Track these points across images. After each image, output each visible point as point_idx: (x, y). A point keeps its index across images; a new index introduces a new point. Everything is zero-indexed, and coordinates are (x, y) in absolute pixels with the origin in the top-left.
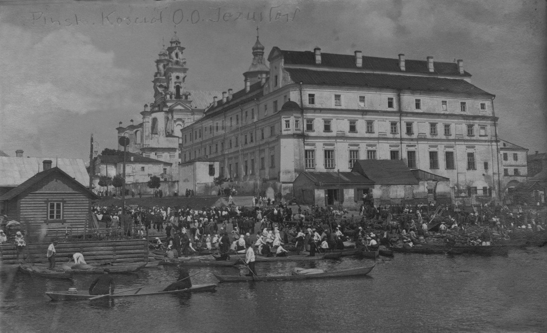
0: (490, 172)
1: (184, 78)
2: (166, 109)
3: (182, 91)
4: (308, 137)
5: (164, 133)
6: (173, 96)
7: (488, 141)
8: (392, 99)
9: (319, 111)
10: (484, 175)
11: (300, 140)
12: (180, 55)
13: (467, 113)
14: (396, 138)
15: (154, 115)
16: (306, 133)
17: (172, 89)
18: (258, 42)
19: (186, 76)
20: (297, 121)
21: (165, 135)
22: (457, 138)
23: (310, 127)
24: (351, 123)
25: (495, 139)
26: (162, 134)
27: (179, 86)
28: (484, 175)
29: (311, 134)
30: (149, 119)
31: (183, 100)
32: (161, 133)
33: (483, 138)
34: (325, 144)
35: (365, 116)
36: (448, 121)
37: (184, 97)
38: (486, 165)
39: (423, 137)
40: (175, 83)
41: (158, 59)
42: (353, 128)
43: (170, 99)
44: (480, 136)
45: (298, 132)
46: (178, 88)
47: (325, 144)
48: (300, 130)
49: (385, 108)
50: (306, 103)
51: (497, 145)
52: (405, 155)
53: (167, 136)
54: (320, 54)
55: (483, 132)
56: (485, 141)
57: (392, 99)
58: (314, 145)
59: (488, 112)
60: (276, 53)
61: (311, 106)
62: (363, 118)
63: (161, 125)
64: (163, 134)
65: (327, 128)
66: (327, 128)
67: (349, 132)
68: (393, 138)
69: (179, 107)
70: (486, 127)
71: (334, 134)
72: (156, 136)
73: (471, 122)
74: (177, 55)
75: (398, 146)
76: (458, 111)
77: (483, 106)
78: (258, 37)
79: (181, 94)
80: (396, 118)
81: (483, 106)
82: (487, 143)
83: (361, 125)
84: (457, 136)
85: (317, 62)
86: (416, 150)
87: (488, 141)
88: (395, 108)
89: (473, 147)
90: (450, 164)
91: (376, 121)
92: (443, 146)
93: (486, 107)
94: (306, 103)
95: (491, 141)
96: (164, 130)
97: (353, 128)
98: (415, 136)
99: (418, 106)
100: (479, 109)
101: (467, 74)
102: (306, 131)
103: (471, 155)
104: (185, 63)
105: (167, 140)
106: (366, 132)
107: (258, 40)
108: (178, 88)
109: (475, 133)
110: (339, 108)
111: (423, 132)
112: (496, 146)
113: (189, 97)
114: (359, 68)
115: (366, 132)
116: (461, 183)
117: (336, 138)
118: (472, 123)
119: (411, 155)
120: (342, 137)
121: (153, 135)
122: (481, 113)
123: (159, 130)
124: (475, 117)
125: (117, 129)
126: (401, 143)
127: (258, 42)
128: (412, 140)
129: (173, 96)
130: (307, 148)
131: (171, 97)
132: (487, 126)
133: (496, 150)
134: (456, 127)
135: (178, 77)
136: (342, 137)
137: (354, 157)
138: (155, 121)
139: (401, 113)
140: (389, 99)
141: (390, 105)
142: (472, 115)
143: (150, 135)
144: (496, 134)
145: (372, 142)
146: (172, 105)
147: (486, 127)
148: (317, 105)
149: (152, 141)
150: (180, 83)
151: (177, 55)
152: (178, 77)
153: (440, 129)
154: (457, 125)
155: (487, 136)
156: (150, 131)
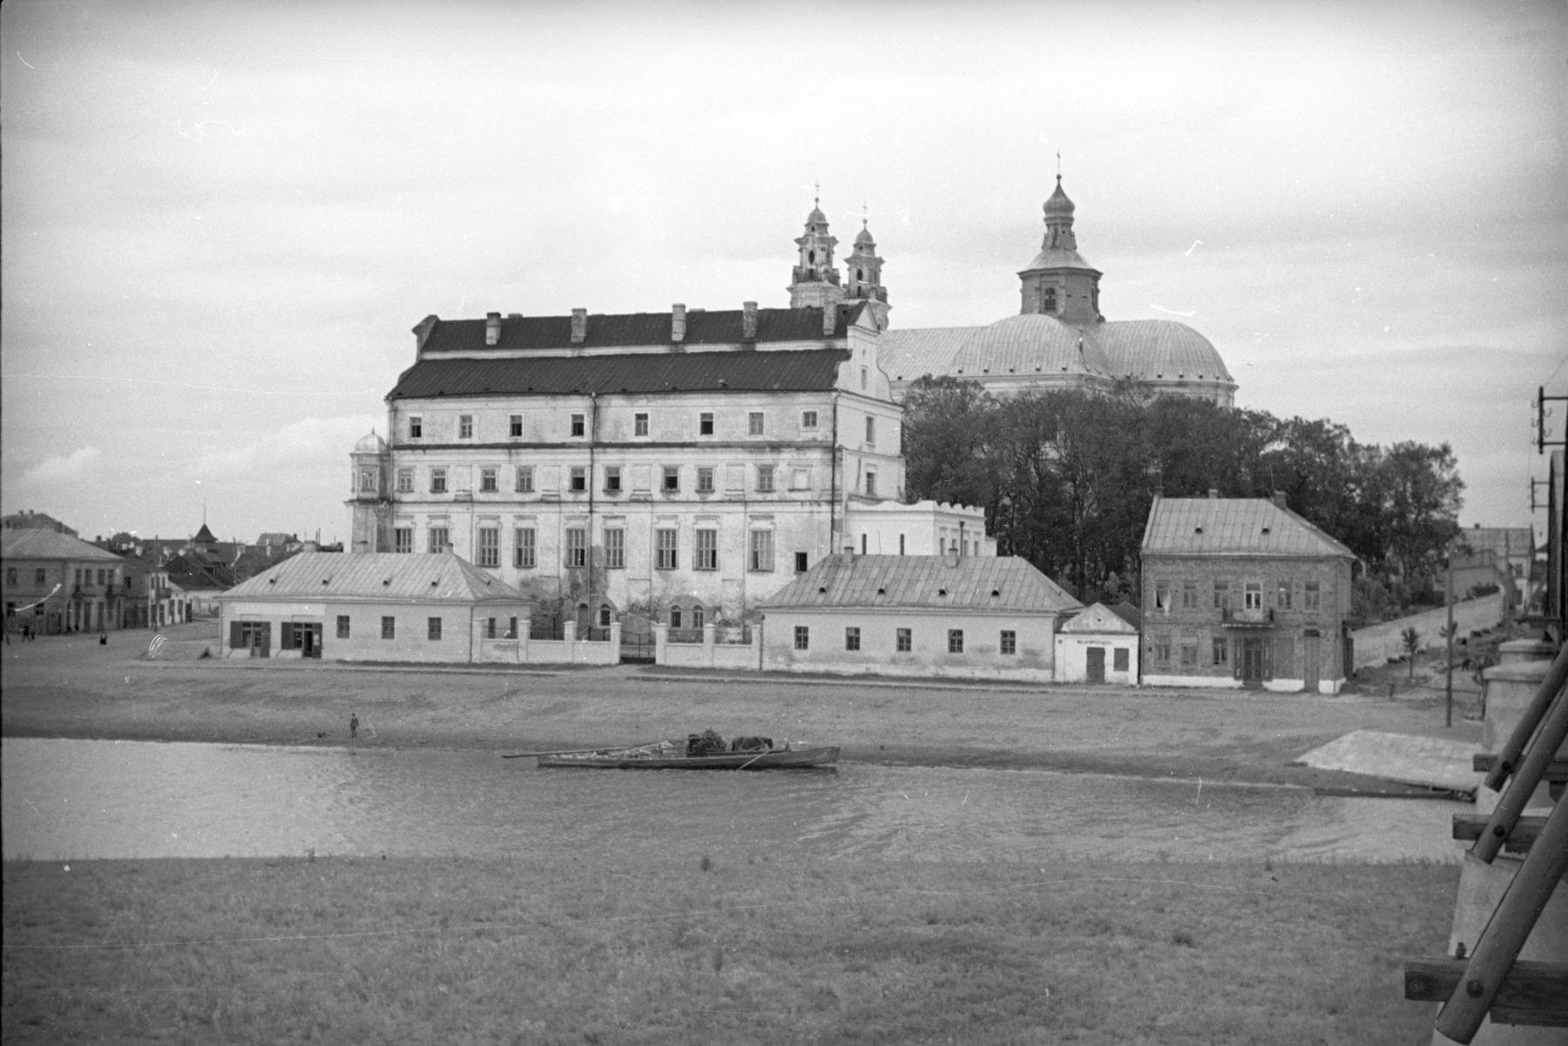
4: (400, 502)
7: (811, 502)
8: (582, 417)
9: (421, 452)
11: (371, 511)
14: (581, 502)
16: (397, 496)
18: (1059, 191)
22: (728, 498)
24: (486, 473)
25: (829, 498)
33: (795, 496)
34: (431, 517)
35: (514, 458)
38: (802, 561)
39: (642, 498)
42: (489, 484)
44: (792, 490)
45: (368, 495)
48: (374, 490)
50: (406, 439)
51: (833, 512)
52: (598, 540)
55: (801, 481)
56: (802, 502)
57: (582, 417)
59: (821, 432)
62: (510, 462)
65: (439, 485)
66: (439, 485)
67: (481, 491)
68: (575, 502)
71: (450, 496)
73: (768, 458)
76: (742, 433)
78: (1059, 177)
80: (581, 458)
81: (810, 419)
82: (807, 508)
84: (729, 493)
85: (488, 342)
86: (625, 527)
87: (811, 502)
88: (587, 437)
89: (770, 517)
90: (708, 560)
91: (539, 466)
92: (691, 518)
95: (818, 503)
97: (489, 484)
98: (625, 495)
100: (797, 426)
106: (517, 491)
109: (777, 485)
110: (466, 441)
111: (643, 486)
112: (829, 515)
115: (517, 491)
117: (456, 501)
118: (771, 462)
119: (615, 537)
120: (468, 501)
122: (806, 435)
124: (776, 447)
126: (591, 512)
127: (1059, 191)
128: (615, 503)
132: (812, 466)
133: (830, 524)
134: (728, 473)
136: (468, 501)
137: (490, 543)
139: (595, 445)
140: (575, 417)
141: (578, 429)
142: (773, 440)
145: (527, 510)
148: (423, 441)
154: (730, 468)
155: (809, 489)
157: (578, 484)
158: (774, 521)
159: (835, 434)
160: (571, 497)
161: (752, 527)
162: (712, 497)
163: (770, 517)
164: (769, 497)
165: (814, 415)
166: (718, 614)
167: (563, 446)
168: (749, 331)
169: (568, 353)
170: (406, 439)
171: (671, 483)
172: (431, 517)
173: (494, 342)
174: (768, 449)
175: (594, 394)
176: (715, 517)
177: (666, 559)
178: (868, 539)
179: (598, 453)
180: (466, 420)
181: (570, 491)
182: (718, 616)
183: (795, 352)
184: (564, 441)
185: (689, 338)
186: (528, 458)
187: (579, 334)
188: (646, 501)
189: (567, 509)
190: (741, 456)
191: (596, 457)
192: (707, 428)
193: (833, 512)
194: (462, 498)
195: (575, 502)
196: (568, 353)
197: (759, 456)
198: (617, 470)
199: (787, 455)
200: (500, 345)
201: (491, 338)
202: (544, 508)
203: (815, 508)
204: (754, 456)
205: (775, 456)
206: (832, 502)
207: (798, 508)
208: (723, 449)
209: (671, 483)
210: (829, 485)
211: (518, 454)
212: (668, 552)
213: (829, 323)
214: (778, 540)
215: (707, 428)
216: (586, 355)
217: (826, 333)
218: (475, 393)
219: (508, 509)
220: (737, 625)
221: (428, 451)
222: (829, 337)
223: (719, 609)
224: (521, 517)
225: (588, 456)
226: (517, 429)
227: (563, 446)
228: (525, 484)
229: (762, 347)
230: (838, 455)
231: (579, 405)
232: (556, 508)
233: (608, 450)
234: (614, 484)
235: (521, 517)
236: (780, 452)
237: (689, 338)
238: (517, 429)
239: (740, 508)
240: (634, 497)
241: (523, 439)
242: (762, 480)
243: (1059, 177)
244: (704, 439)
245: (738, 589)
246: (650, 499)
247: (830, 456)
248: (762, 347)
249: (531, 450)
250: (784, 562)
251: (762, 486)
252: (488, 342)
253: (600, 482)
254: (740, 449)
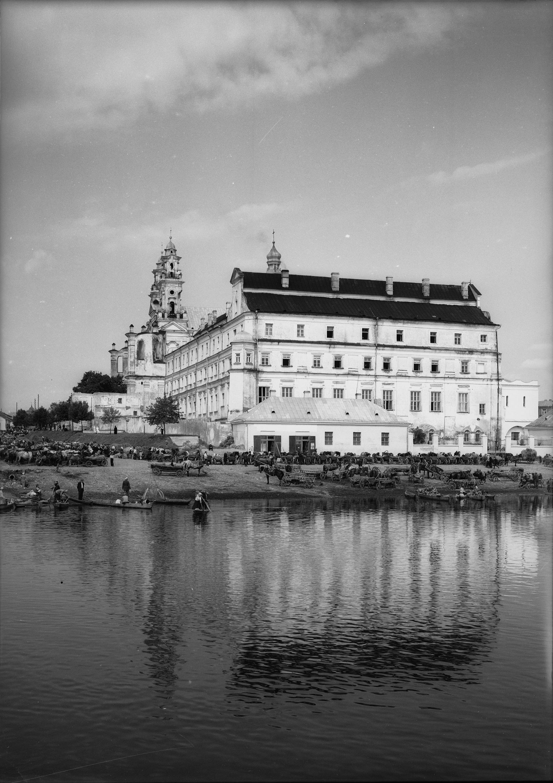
0: (487, 417)
1: (179, 294)
2: (155, 330)
3: (177, 308)
5: (152, 359)
6: (166, 315)
9: (277, 343)
10: (478, 419)
11: (252, 375)
12: (176, 266)
13: (463, 346)
15: (141, 337)
16: (260, 368)
17: (166, 306)
18: (274, 249)
19: (182, 291)
20: (249, 355)
21: (153, 361)
22: (447, 376)
23: (265, 362)
25: (496, 378)
26: (149, 360)
27: (173, 302)
28: (478, 419)
29: (265, 369)
30: (135, 341)
31: (177, 319)
32: (149, 359)
35: (331, 349)
37: (178, 316)
38: (482, 408)
39: (403, 374)
40: (169, 299)
41: (156, 269)
42: (317, 364)
43: (162, 319)
44: (477, 373)
46: (172, 305)
47: (282, 381)
49: (358, 339)
51: (498, 385)
53: (155, 362)
54: (288, 276)
55: (481, 369)
58: (269, 381)
59: (490, 345)
60: (237, 275)
63: (148, 349)
64: (151, 360)
65: (286, 363)
68: (366, 375)
69: (173, 328)
70: (485, 363)
71: (294, 369)
72: (143, 362)
73: (466, 357)
74: (172, 265)
75: (372, 384)
76: (451, 344)
77: (483, 338)
78: (274, 243)
79: (175, 312)
80: (370, 352)
81: (483, 338)
82: (485, 382)
83: (328, 361)
84: (447, 373)
85: (284, 286)
86: (393, 389)
88: (371, 339)
89: (467, 386)
92: (428, 385)
93: (488, 338)
95: (491, 380)
96: (152, 355)
97: (317, 364)
99: (399, 337)
102: (260, 365)
103: (464, 396)
104: (181, 274)
105: (155, 367)
107: (274, 246)
108: (172, 305)
109: (470, 370)
113: (184, 315)
116: (449, 428)
119: (388, 393)
121: (139, 361)
122: (482, 346)
123: (146, 355)
124: (471, 352)
125: (110, 351)
127: (274, 249)
128: (389, 377)
129: (166, 315)
130: (261, 384)
131: (163, 316)
132: (487, 362)
135: (172, 292)
138: (141, 343)
139: (378, 346)
143: (136, 360)
144: (498, 372)
145: (340, 379)
146: (165, 325)
147: (485, 363)
149: (138, 367)
150: (175, 298)
151: (172, 265)
152: (172, 292)
156: (136, 356)
157: (367, 366)
158: (469, 388)
159: (497, 346)
161: (458, 391)
162: (438, 375)
163: (467, 386)
164: (467, 376)
165: (485, 336)
166: (442, 434)
167: (358, 345)
168: (427, 294)
169: (330, 296)
170: (263, 336)
171: (417, 367)
172: (282, 381)
173: (287, 286)
174: (467, 353)
175: (378, 318)
176: (440, 385)
177: (415, 406)
178: (526, 398)
179: (379, 349)
180: (300, 327)
181: (363, 369)
182: (442, 435)
183: (437, 305)
184: (358, 342)
185: (396, 294)
186: (339, 350)
187: (336, 286)
188: (406, 376)
189: (362, 378)
190: (454, 355)
192: (433, 340)
193: (498, 385)
194: (302, 371)
195: (366, 375)
196: (330, 296)
197: (462, 356)
198: (389, 359)
199: (475, 356)
200: (290, 288)
201: (286, 284)
202: (351, 378)
203: (489, 382)
204: (459, 355)
205: (469, 356)
206: (498, 380)
207: (481, 382)
208: (445, 351)
209: (417, 367)
210: (496, 372)
211: (334, 348)
212: (436, 403)
213: (465, 293)
214: (471, 398)
215: (433, 340)
216: (341, 298)
217: (465, 298)
218: (297, 312)
220: (453, 439)
221: (280, 343)
222: (466, 300)
223: (442, 431)
224: (337, 383)
226: (330, 334)
227: (358, 345)
228: (337, 364)
229: (433, 302)
230: (499, 357)
231: (367, 323)
232: (356, 378)
233: (386, 348)
234: (386, 366)
235: (337, 383)
236: (472, 354)
237: (396, 294)
238: (330, 334)
239: (453, 381)
240: (400, 374)
241: (335, 339)
242: (463, 367)
243: (274, 243)
244: (432, 345)
245: (453, 421)
246: (407, 375)
247: (496, 358)
248: (433, 302)
249: (343, 346)
250: (474, 408)
251: (463, 371)
252: (284, 286)
253: (381, 366)
254: (453, 352)
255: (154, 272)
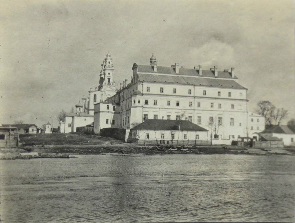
29: (146, 106)
30: (92, 95)
36: (220, 101)
59: (244, 97)
61: (148, 93)
65: (155, 104)
80: (192, 100)
94: (145, 92)
101: (236, 78)
114: (177, 74)
131: (105, 84)
138: (95, 96)
151: (109, 62)
153: (216, 106)
160: (189, 108)
169: (175, 76)
191: (195, 99)
196: (175, 76)
219: (173, 110)
225: (193, 99)
231: (191, 88)
255: (102, 65)
